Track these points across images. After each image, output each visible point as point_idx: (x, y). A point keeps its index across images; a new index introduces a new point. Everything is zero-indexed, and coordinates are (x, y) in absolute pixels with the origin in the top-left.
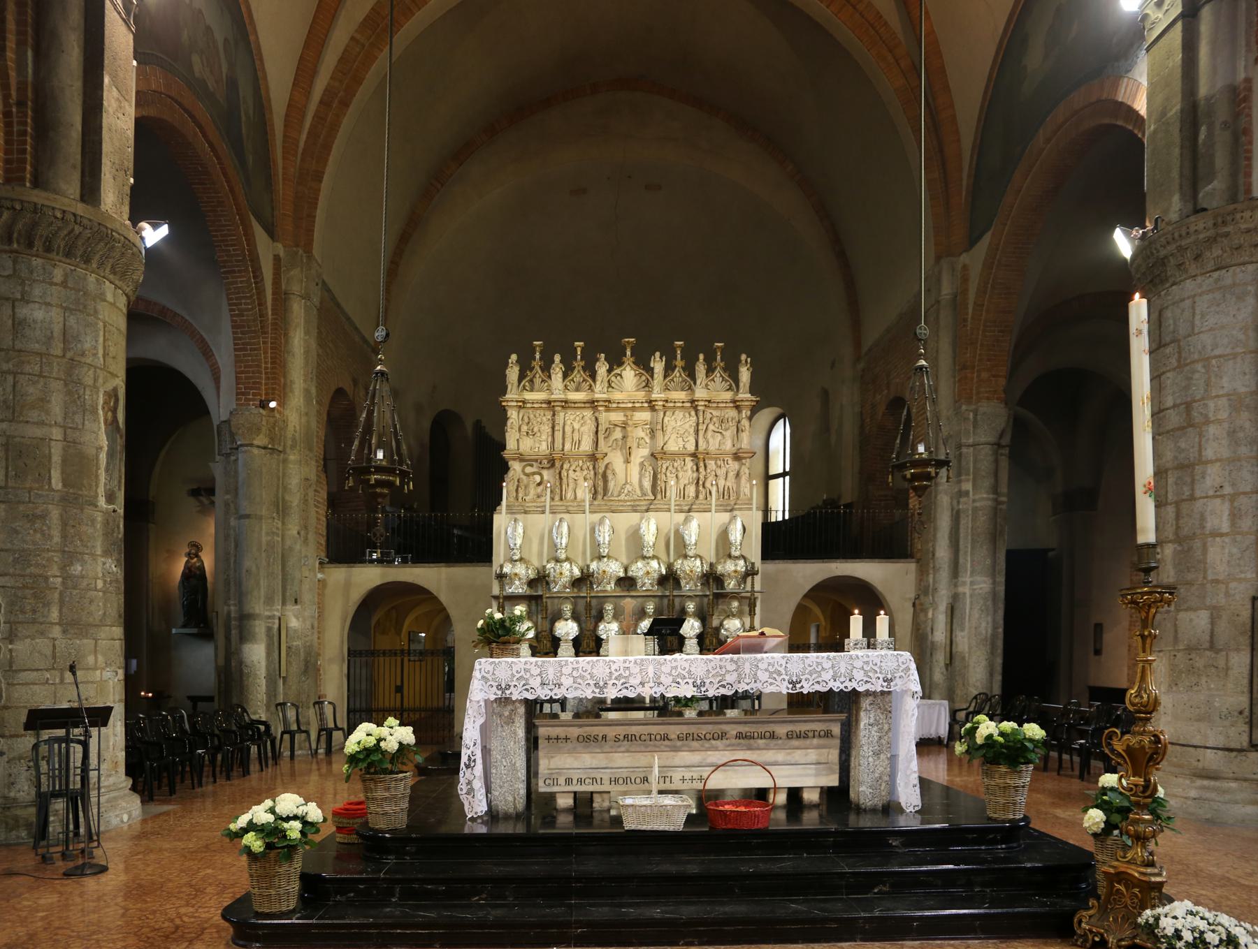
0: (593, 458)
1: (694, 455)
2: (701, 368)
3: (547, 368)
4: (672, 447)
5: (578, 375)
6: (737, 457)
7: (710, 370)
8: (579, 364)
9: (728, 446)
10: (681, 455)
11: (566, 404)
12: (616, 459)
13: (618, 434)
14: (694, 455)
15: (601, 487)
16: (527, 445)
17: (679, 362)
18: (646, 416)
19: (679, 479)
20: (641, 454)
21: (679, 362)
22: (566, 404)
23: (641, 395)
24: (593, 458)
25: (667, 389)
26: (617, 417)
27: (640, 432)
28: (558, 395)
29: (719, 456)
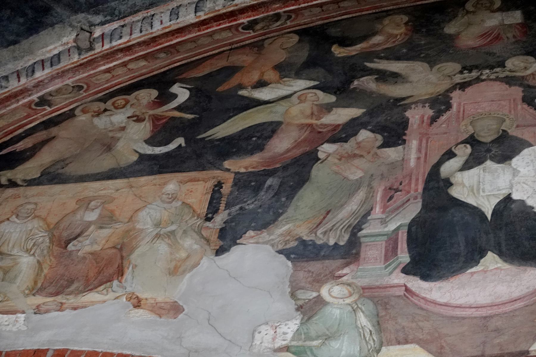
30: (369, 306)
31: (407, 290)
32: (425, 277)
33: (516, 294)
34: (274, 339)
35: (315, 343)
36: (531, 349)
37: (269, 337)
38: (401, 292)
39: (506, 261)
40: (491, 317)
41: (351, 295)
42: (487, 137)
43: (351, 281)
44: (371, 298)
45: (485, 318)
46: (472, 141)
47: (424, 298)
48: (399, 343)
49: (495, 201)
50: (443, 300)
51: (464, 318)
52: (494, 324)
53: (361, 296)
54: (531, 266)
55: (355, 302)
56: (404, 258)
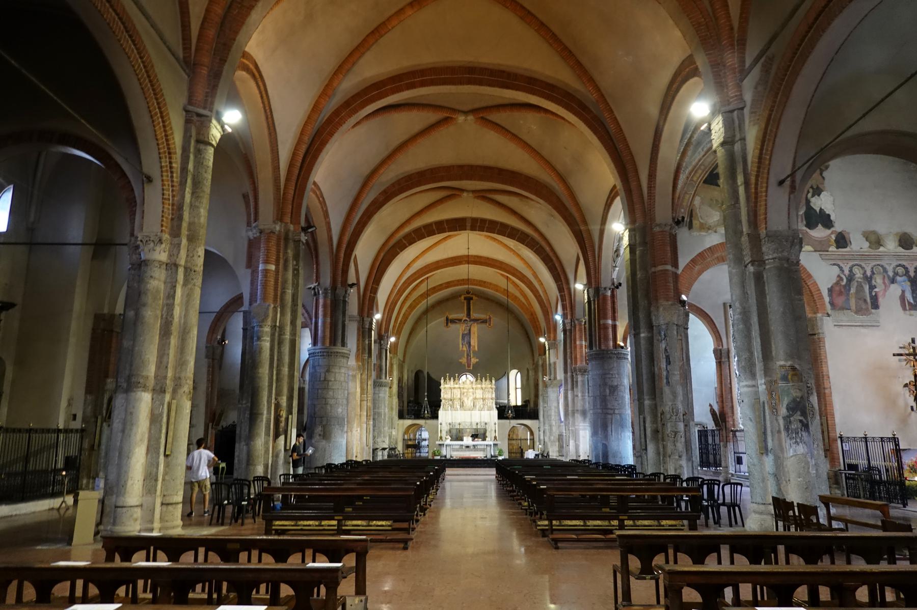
0: (460, 399)
1: (482, 399)
2: (484, 380)
3: (450, 379)
4: (477, 397)
5: (457, 381)
6: (492, 399)
7: (486, 380)
8: (457, 379)
9: (490, 397)
10: (480, 399)
11: (454, 388)
12: (465, 399)
13: (465, 394)
14: (482, 399)
15: (462, 405)
16: (445, 396)
17: (479, 378)
18: (472, 390)
19: (479, 403)
20: (471, 398)
21: (479, 378)
22: (454, 388)
23: (470, 386)
24: (460, 399)
25: (476, 384)
26: (465, 390)
27: (471, 394)
28: (452, 386)
29: (488, 399)
32: (809, 229)
40: (821, 241)
42: (815, 187)
46: (812, 187)
49: (819, 209)
56: (805, 222)
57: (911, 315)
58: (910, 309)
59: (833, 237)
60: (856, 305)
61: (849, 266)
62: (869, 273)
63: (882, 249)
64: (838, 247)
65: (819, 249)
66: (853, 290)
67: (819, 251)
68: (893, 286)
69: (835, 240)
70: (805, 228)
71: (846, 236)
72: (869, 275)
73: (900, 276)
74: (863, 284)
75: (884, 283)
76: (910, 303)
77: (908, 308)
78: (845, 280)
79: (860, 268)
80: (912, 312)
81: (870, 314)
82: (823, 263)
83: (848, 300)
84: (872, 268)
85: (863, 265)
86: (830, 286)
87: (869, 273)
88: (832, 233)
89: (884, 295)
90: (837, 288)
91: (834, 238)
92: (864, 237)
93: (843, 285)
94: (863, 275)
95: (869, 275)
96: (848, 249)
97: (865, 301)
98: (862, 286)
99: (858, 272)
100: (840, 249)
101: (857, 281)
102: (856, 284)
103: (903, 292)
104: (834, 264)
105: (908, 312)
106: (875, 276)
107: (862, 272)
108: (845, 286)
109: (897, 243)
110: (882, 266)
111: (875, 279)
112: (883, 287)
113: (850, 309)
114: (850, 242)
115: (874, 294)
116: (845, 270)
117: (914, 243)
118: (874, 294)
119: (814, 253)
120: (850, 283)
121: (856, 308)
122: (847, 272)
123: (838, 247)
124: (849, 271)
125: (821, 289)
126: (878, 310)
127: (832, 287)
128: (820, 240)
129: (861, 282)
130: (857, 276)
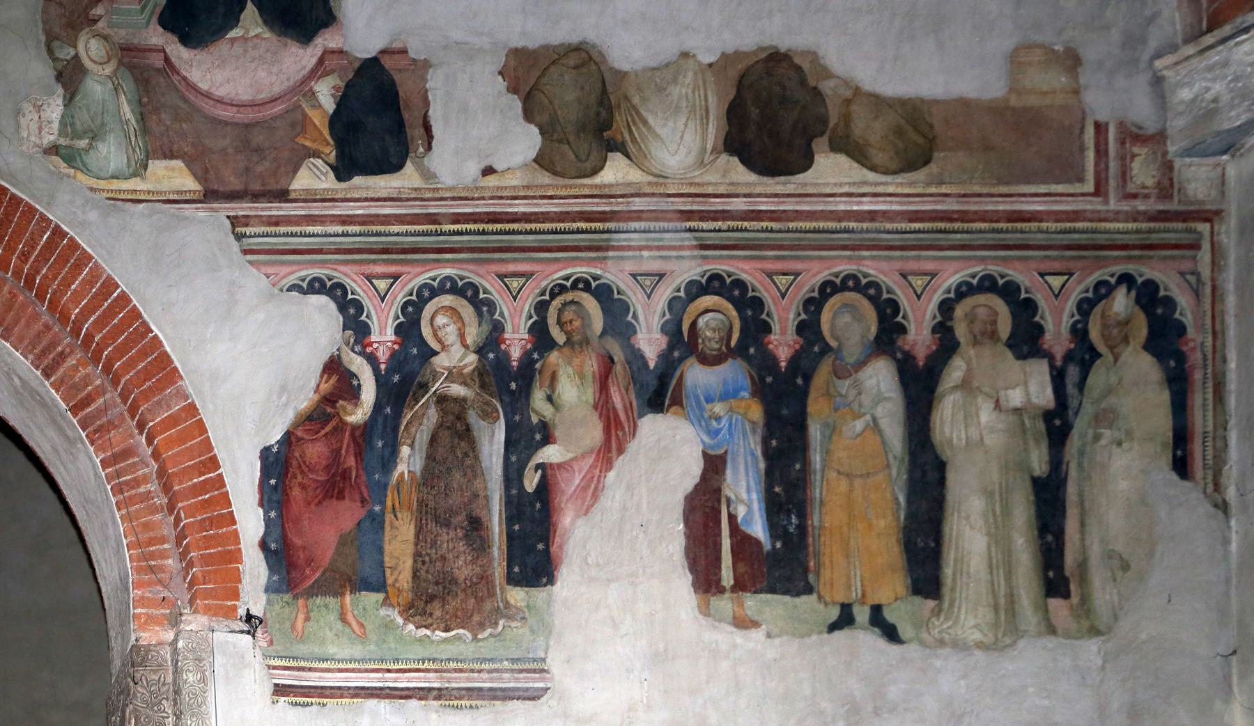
30: (128, 84)
31: (167, 60)
33: (277, 90)
34: (40, 129)
35: (83, 143)
36: (291, 188)
37: (34, 127)
38: (159, 63)
39: (266, 22)
41: (109, 60)
43: (108, 31)
44: (131, 68)
45: (247, 126)
47: (184, 79)
48: (165, 157)
50: (204, 86)
51: (226, 123)
52: (258, 138)
53: (121, 63)
54: (292, 39)
55: (115, 72)
57: (743, 623)
58: (740, 586)
59: (326, 94)
60: (417, 555)
61: (400, 295)
62: (516, 341)
63: (615, 171)
64: (344, 170)
65: (235, 184)
66: (409, 461)
67: (232, 196)
68: (653, 428)
69: (334, 120)
70: (157, 37)
71: (405, 86)
72: (516, 353)
73: (706, 360)
74: (473, 418)
75: (603, 407)
76: (743, 542)
77: (727, 577)
78: (369, 394)
79: (467, 311)
80: (752, 603)
81: (497, 613)
82: (253, 281)
83: (376, 523)
84: (542, 307)
85: (491, 287)
86: (275, 436)
87: (516, 341)
88: (319, 70)
89: (592, 491)
90: (316, 451)
91: (329, 105)
92: (513, 89)
93: (355, 428)
94: (480, 351)
95: (516, 353)
96: (407, 179)
97: (476, 525)
98: (466, 435)
99: (451, 334)
100: (357, 180)
101: (442, 400)
102: (432, 416)
103: (714, 465)
104: (316, 287)
105: (724, 604)
106: (554, 357)
107: (474, 334)
108: (365, 432)
109: (714, 130)
110: (604, 293)
111: (554, 378)
112: (593, 433)
113: (378, 585)
114: (428, 129)
115: (531, 482)
116: (375, 326)
117: (824, 121)
118: (531, 482)
119: (200, 213)
120: (398, 415)
121: (415, 575)
122: (384, 337)
123: (344, 170)
124: (399, 330)
125: (222, 456)
126: (539, 594)
127: (289, 439)
128: (249, 116)
129: (461, 401)
130: (442, 362)
